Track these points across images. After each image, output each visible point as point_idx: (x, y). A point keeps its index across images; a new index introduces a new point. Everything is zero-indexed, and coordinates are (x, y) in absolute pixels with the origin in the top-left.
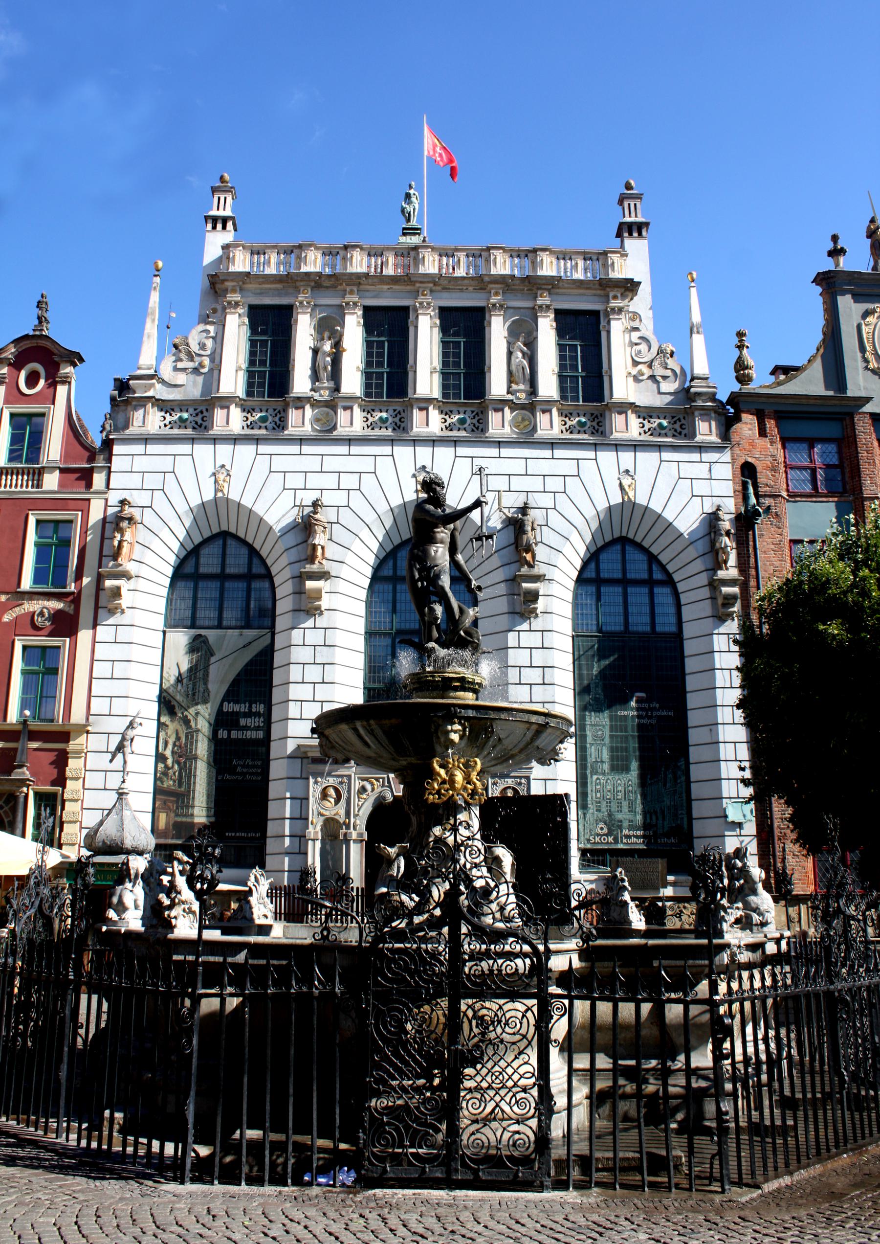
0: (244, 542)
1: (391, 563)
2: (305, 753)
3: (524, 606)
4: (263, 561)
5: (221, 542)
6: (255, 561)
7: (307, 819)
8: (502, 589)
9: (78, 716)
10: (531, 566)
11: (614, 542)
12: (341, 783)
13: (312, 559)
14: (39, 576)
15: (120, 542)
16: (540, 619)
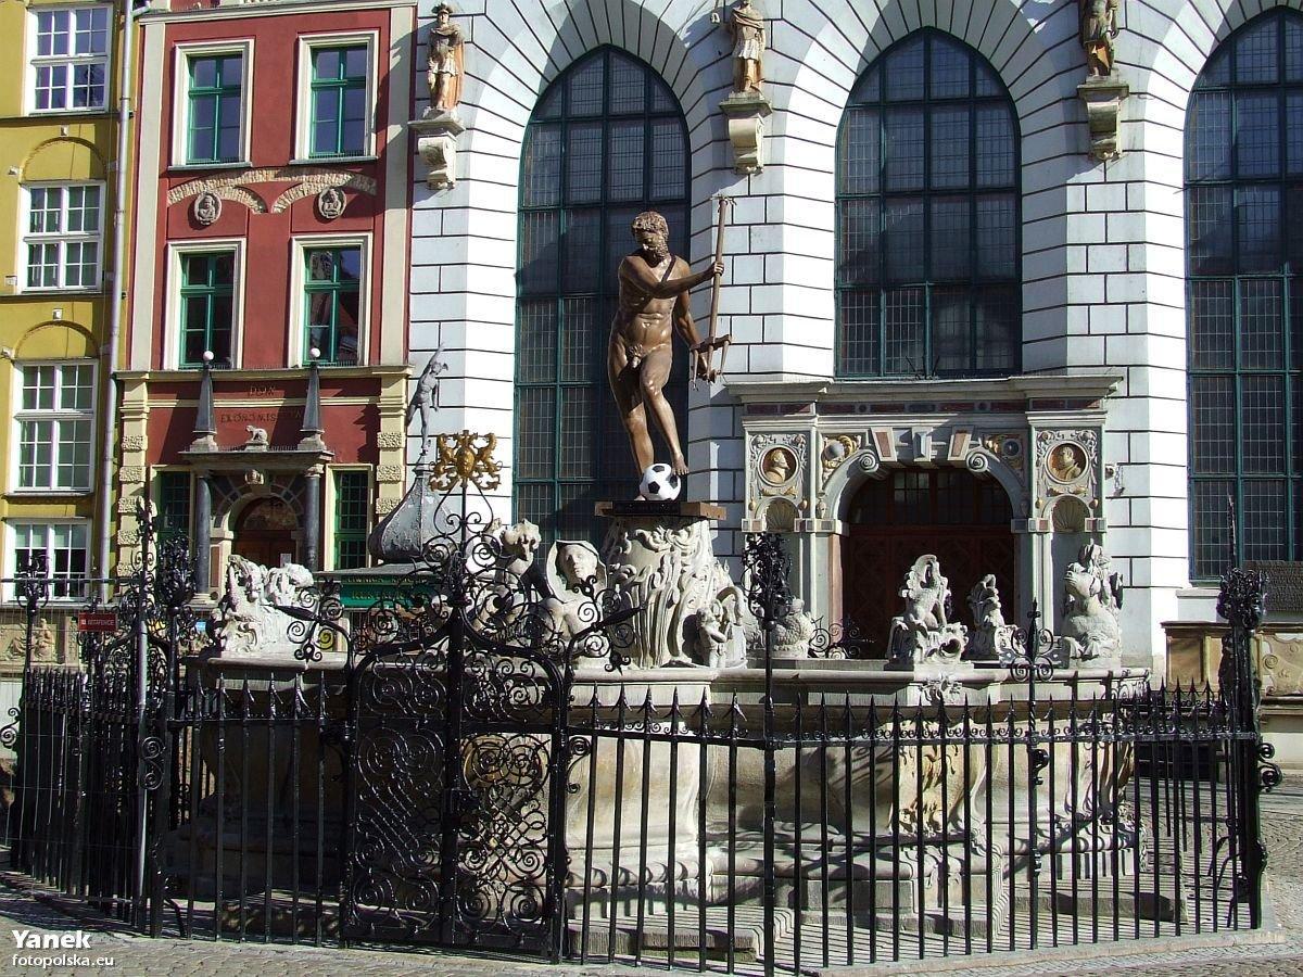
0: (635, 60)
1: (877, 79)
2: (738, 397)
3: (1092, 139)
4: (668, 90)
5: (600, 63)
6: (657, 90)
7: (743, 501)
8: (1057, 114)
9: (391, 354)
10: (1105, 71)
11: (1264, 16)
12: (795, 443)
13: (739, 82)
14: (322, 138)
15: (439, 76)
16: (1122, 163)
